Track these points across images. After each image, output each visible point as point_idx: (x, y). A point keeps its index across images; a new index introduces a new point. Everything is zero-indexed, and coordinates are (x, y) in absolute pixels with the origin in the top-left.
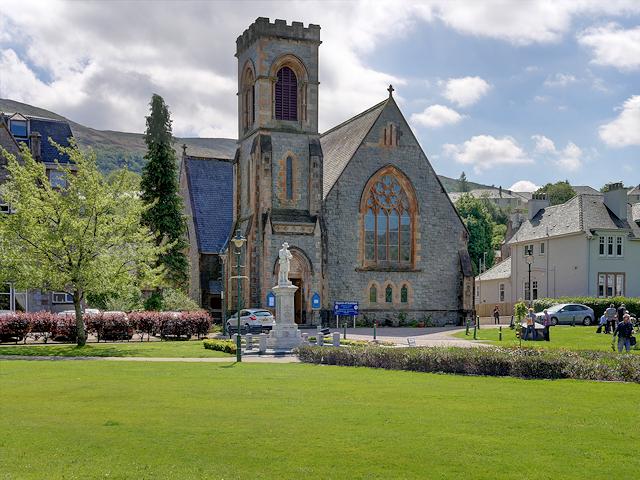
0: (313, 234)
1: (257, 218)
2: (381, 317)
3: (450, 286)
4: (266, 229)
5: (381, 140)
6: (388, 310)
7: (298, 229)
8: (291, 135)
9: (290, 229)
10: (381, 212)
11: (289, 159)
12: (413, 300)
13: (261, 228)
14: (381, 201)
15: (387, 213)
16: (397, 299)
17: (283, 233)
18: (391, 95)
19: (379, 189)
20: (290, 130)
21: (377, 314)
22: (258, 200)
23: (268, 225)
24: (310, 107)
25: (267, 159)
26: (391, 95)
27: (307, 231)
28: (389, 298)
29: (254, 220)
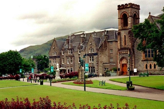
0: (127, 53)
6: (150, 71)
7: (124, 52)
9: (123, 53)
11: (125, 36)
17: (121, 54)
18: (150, 14)
27: (126, 53)
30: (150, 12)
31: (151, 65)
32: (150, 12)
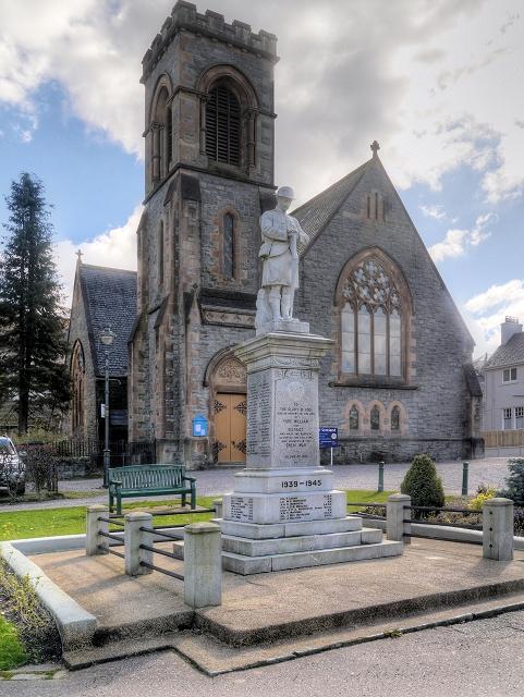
1: (175, 300)
2: (365, 449)
3: (452, 409)
4: (191, 316)
5: (363, 211)
8: (232, 183)
9: (231, 319)
10: (364, 307)
11: (230, 216)
12: (406, 427)
13: (181, 315)
14: (364, 292)
15: (371, 309)
16: (386, 426)
18: (375, 155)
19: (360, 276)
20: (229, 176)
21: (361, 445)
22: (176, 272)
23: (195, 309)
24: (260, 146)
25: (192, 210)
26: (375, 155)
28: (375, 426)
29: (170, 303)
30: (375, 142)
31: (375, 413)
32: (375, 142)
